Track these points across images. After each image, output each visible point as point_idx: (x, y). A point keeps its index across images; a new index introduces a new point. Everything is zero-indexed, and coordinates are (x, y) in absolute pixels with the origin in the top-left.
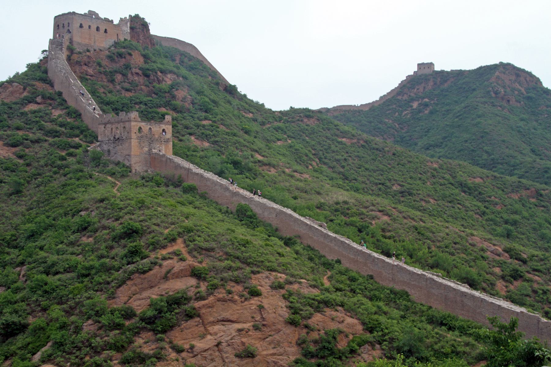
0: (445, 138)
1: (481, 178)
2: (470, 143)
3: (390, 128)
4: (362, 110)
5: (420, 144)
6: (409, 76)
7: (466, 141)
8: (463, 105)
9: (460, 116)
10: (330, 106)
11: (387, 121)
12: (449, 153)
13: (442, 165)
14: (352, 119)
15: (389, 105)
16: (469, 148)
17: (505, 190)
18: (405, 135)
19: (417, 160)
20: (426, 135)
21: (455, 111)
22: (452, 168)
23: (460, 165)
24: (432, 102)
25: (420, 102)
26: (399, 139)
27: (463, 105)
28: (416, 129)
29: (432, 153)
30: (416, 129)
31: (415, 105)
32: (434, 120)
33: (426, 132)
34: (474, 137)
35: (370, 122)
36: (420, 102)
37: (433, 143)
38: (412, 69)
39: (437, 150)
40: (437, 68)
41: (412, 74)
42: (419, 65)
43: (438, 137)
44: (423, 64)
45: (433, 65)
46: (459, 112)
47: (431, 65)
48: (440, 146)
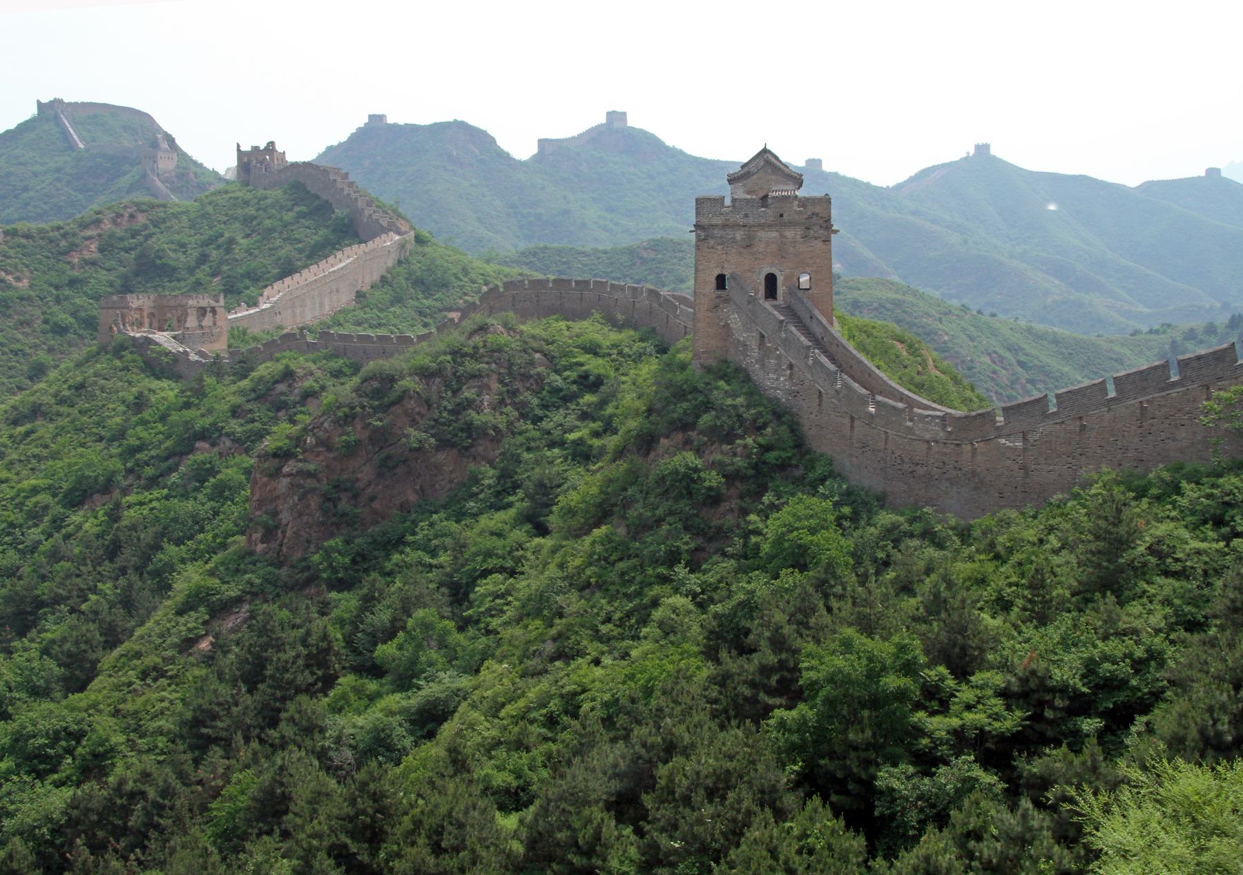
38: (362, 121)
40: (390, 121)
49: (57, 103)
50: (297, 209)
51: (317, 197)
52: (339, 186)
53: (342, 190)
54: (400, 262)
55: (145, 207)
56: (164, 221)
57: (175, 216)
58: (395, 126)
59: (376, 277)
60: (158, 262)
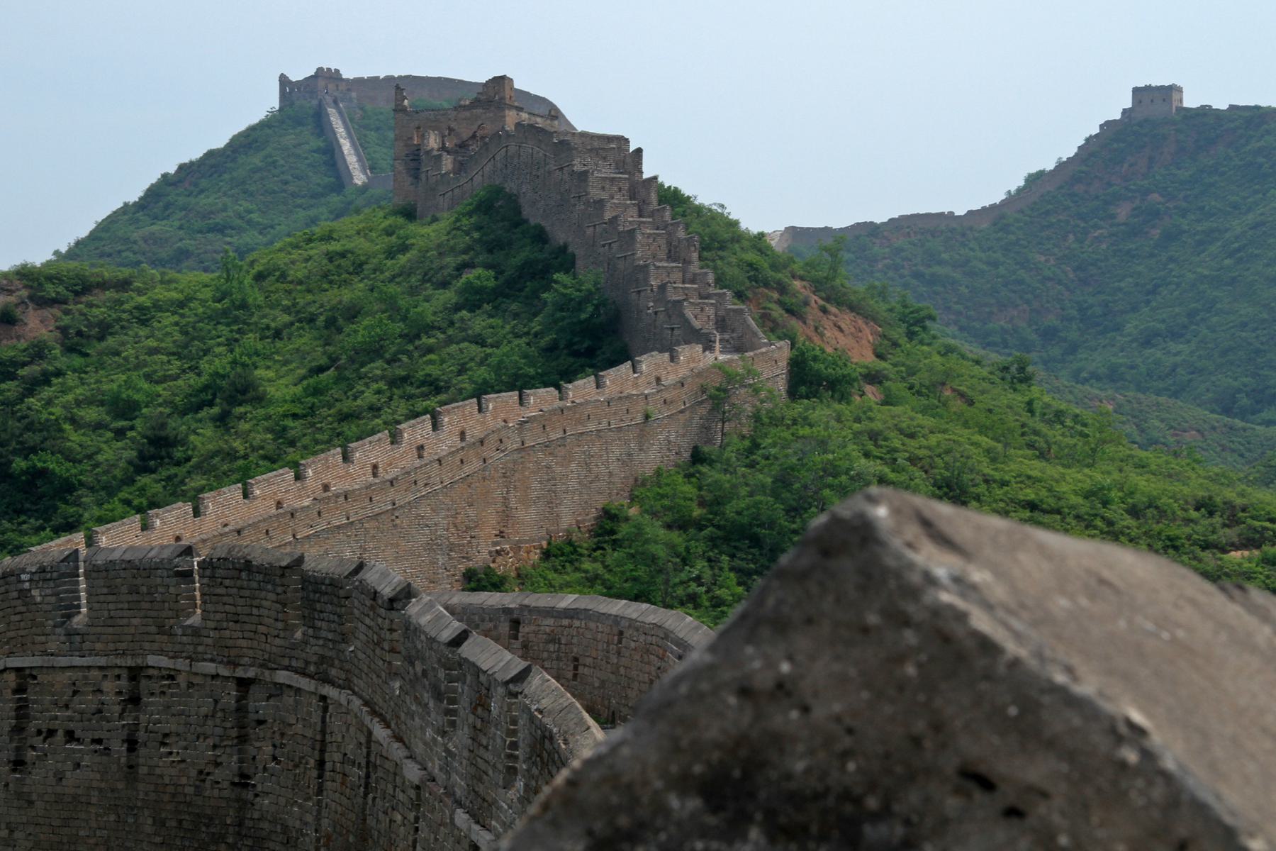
0: (1191, 314)
1: (1198, 431)
2: (1255, 330)
3: (1050, 279)
4: (971, 229)
5: (1129, 328)
6: (1108, 123)
7: (1244, 325)
8: (1250, 218)
9: (1238, 250)
10: (880, 217)
11: (1043, 259)
12: (1200, 357)
13: (1120, 406)
14: (945, 256)
15: (1047, 213)
16: (1250, 344)
17: (1247, 454)
18: (1091, 300)
19: (1071, 397)
20: (1148, 302)
21: (1227, 235)
22: (1141, 411)
23: (1158, 404)
24: (1170, 205)
25: (1137, 202)
26: (1074, 313)
27: (1250, 218)
28: (1122, 285)
29: (1159, 354)
30: (1122, 285)
31: (1123, 212)
32: (1171, 259)
33: (1148, 293)
34: (1265, 316)
35: (995, 264)
36: (1137, 202)
37: (1163, 326)
38: (1116, 104)
39: (1173, 347)
40: (1191, 100)
41: (1118, 116)
42: (1136, 91)
43: (1177, 310)
44: (1148, 88)
45: (1180, 90)
46: (1237, 238)
47: (1170, 92)
48: (1182, 336)
49: (326, 77)
50: (470, 276)
51: (540, 237)
52: (595, 192)
53: (600, 204)
54: (697, 457)
55: (51, 290)
56: (105, 330)
57: (143, 316)
58: (1205, 111)
59: (573, 515)
60: (19, 464)
